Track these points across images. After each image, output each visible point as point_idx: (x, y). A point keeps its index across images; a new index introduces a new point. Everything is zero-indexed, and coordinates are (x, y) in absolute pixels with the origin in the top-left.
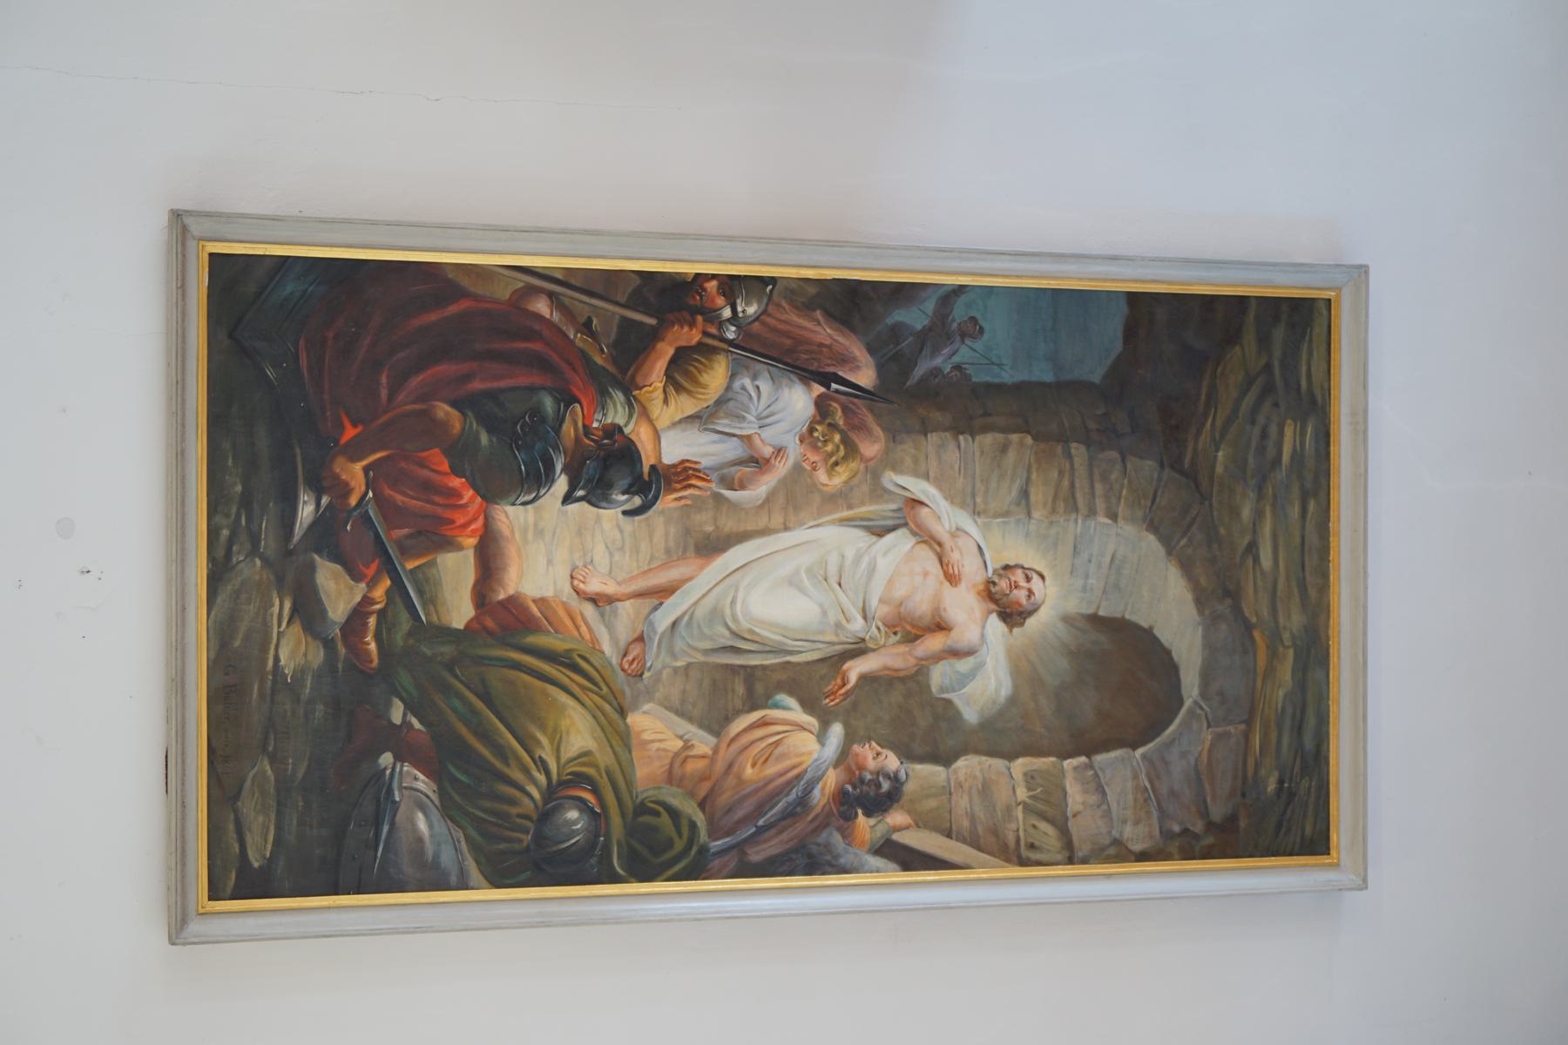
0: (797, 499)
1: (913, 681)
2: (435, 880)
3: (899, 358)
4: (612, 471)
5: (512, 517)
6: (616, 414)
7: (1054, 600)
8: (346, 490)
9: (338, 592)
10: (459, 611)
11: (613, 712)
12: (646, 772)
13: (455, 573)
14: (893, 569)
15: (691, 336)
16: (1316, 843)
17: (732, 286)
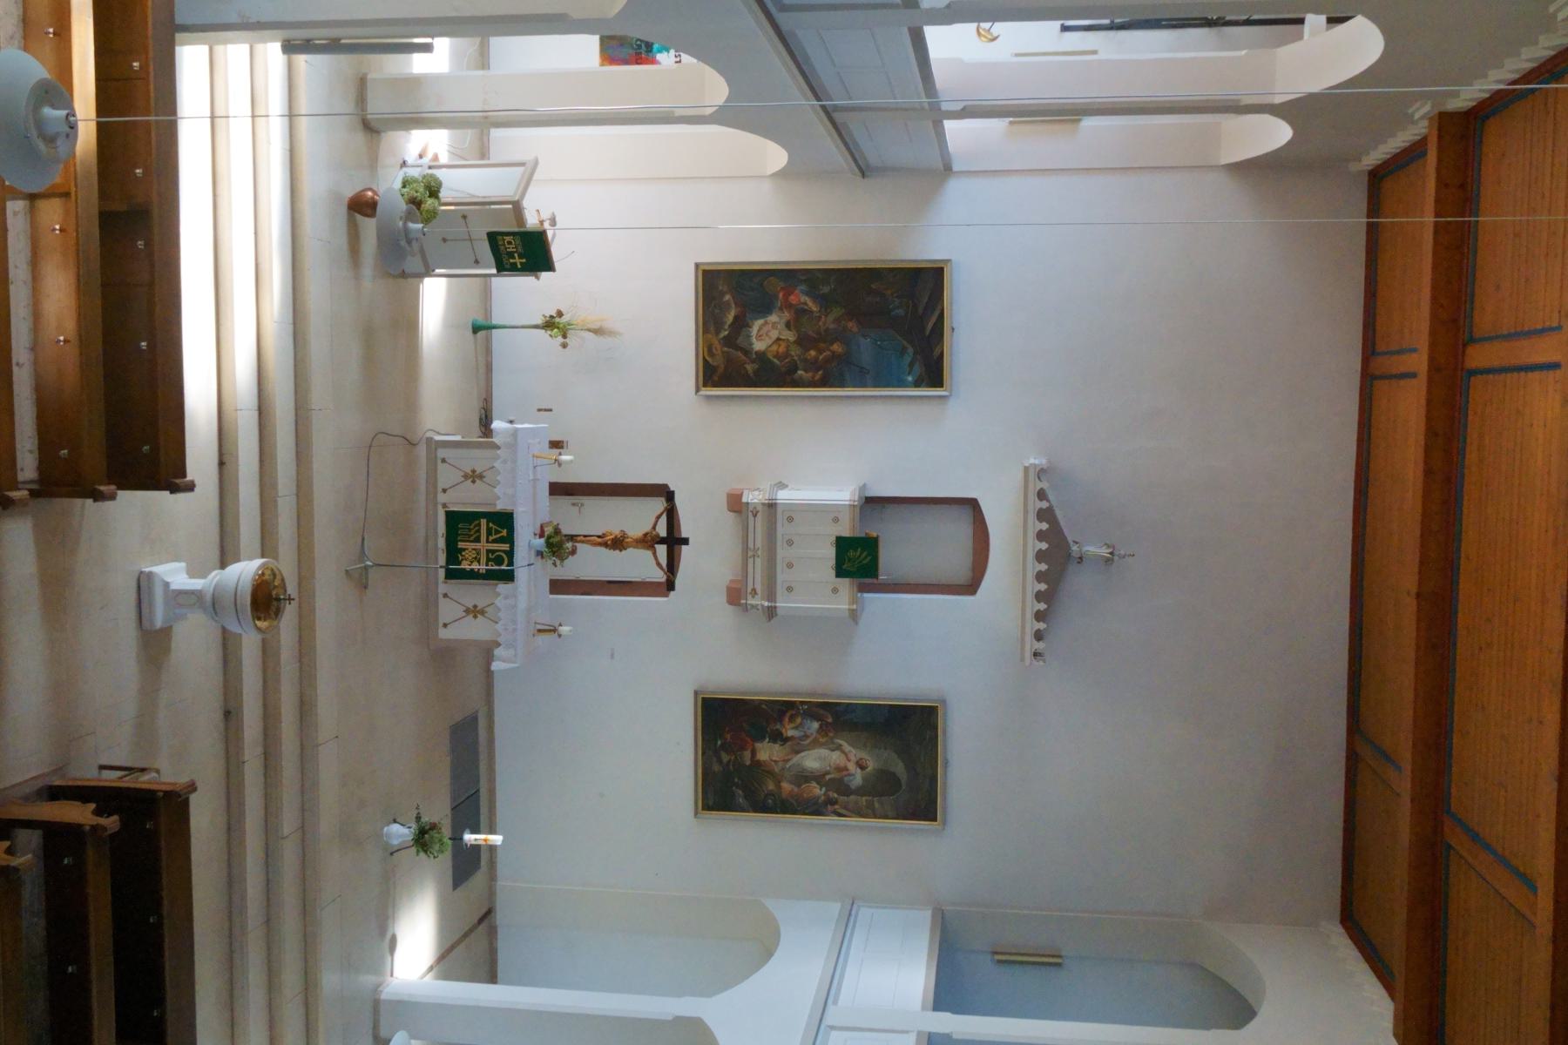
0: (815, 744)
1: (841, 780)
2: (743, 810)
3: (839, 718)
4: (778, 737)
5: (758, 745)
7: (871, 765)
12: (784, 795)
14: (836, 758)
16: (932, 817)
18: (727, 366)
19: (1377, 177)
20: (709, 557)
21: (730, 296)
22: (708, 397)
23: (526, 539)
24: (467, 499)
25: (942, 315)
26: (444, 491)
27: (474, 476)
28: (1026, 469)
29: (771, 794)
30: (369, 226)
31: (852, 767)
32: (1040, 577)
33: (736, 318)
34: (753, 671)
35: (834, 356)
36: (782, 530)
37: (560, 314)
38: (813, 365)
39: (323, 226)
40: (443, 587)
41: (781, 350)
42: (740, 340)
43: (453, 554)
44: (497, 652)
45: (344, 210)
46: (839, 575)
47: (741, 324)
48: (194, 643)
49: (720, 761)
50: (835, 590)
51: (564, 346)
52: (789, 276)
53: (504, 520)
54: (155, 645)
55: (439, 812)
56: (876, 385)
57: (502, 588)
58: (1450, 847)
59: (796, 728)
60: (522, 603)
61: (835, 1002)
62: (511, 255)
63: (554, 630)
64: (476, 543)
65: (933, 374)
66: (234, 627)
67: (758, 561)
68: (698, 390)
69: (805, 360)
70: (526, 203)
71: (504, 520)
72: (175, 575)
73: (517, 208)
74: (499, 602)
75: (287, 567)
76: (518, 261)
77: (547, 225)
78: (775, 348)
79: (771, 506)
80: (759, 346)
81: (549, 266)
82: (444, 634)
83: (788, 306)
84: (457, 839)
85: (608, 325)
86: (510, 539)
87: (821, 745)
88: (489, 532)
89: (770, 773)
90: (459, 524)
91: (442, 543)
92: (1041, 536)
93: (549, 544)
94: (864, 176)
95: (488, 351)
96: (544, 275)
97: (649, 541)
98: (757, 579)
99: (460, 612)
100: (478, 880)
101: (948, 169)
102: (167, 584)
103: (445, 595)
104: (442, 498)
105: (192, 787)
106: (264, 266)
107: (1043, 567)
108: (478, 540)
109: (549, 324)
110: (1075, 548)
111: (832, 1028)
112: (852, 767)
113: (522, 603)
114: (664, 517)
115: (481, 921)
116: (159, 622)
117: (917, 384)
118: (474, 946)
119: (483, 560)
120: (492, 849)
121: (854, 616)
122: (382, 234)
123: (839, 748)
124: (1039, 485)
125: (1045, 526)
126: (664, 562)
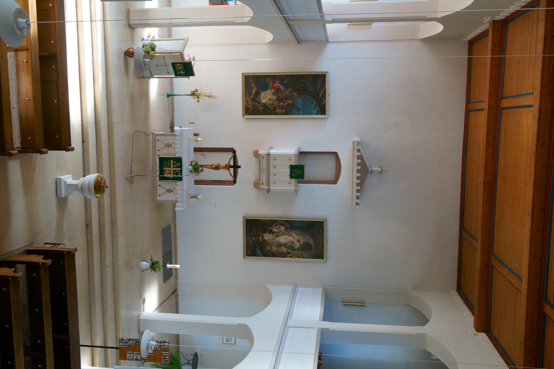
0: (283, 234)
2: (260, 256)
3: (291, 225)
4: (271, 232)
5: (264, 235)
9: (253, 239)
10: (261, 240)
11: (271, 246)
12: (273, 251)
13: (261, 238)
14: (290, 238)
18: (253, 108)
19: (471, 43)
20: (248, 172)
21: (254, 84)
22: (247, 118)
23: (186, 166)
24: (166, 153)
26: (159, 150)
27: (168, 146)
28: (354, 142)
29: (268, 251)
30: (131, 61)
31: (296, 241)
32: (358, 178)
33: (256, 92)
34: (262, 210)
35: (289, 104)
36: (272, 163)
37: (197, 91)
38: (282, 107)
39: (116, 60)
40: (158, 183)
41: (271, 102)
42: (258, 99)
43: (162, 172)
44: (177, 204)
45: (123, 55)
46: (291, 177)
47: (257, 94)
48: (75, 202)
49: (252, 240)
50: (290, 183)
51: (198, 101)
52: (273, 78)
53: (179, 160)
54: (62, 202)
55: (158, 257)
56: (303, 114)
57: (178, 183)
58: (493, 266)
60: (185, 188)
61: (291, 319)
62: (180, 71)
63: (196, 197)
64: (170, 168)
65: (322, 110)
66: (88, 196)
67: (264, 173)
68: (243, 116)
69: (279, 106)
70: (184, 53)
71: (179, 160)
72: (68, 179)
73: (182, 54)
74: (177, 188)
75: (106, 176)
76: (182, 72)
77: (192, 60)
78: (269, 102)
79: (268, 155)
80: (264, 101)
81: (193, 74)
82: (159, 198)
83: (273, 87)
84: (165, 266)
85: (213, 94)
86: (181, 167)
87: (286, 234)
88: (174, 164)
89: (269, 244)
90: (164, 161)
91: (158, 168)
92: (358, 164)
93: (194, 168)
94: (299, 43)
95: (172, 103)
96: (191, 77)
97: (227, 167)
98: (264, 180)
99: (164, 191)
100: (172, 279)
101: (327, 41)
102: (66, 182)
103: (159, 186)
104: (158, 153)
105: (76, 250)
106: (96, 74)
107: (359, 175)
108: (170, 167)
109: (193, 94)
110: (370, 168)
111: (290, 327)
112: (296, 241)
113: (185, 188)
114: (232, 160)
115: (173, 293)
116: (63, 195)
117: (317, 114)
118: (171, 301)
119: (172, 174)
120: (176, 269)
121: (296, 191)
122: (137, 63)
123: (291, 235)
124: (358, 147)
125: (360, 161)
126: (232, 174)
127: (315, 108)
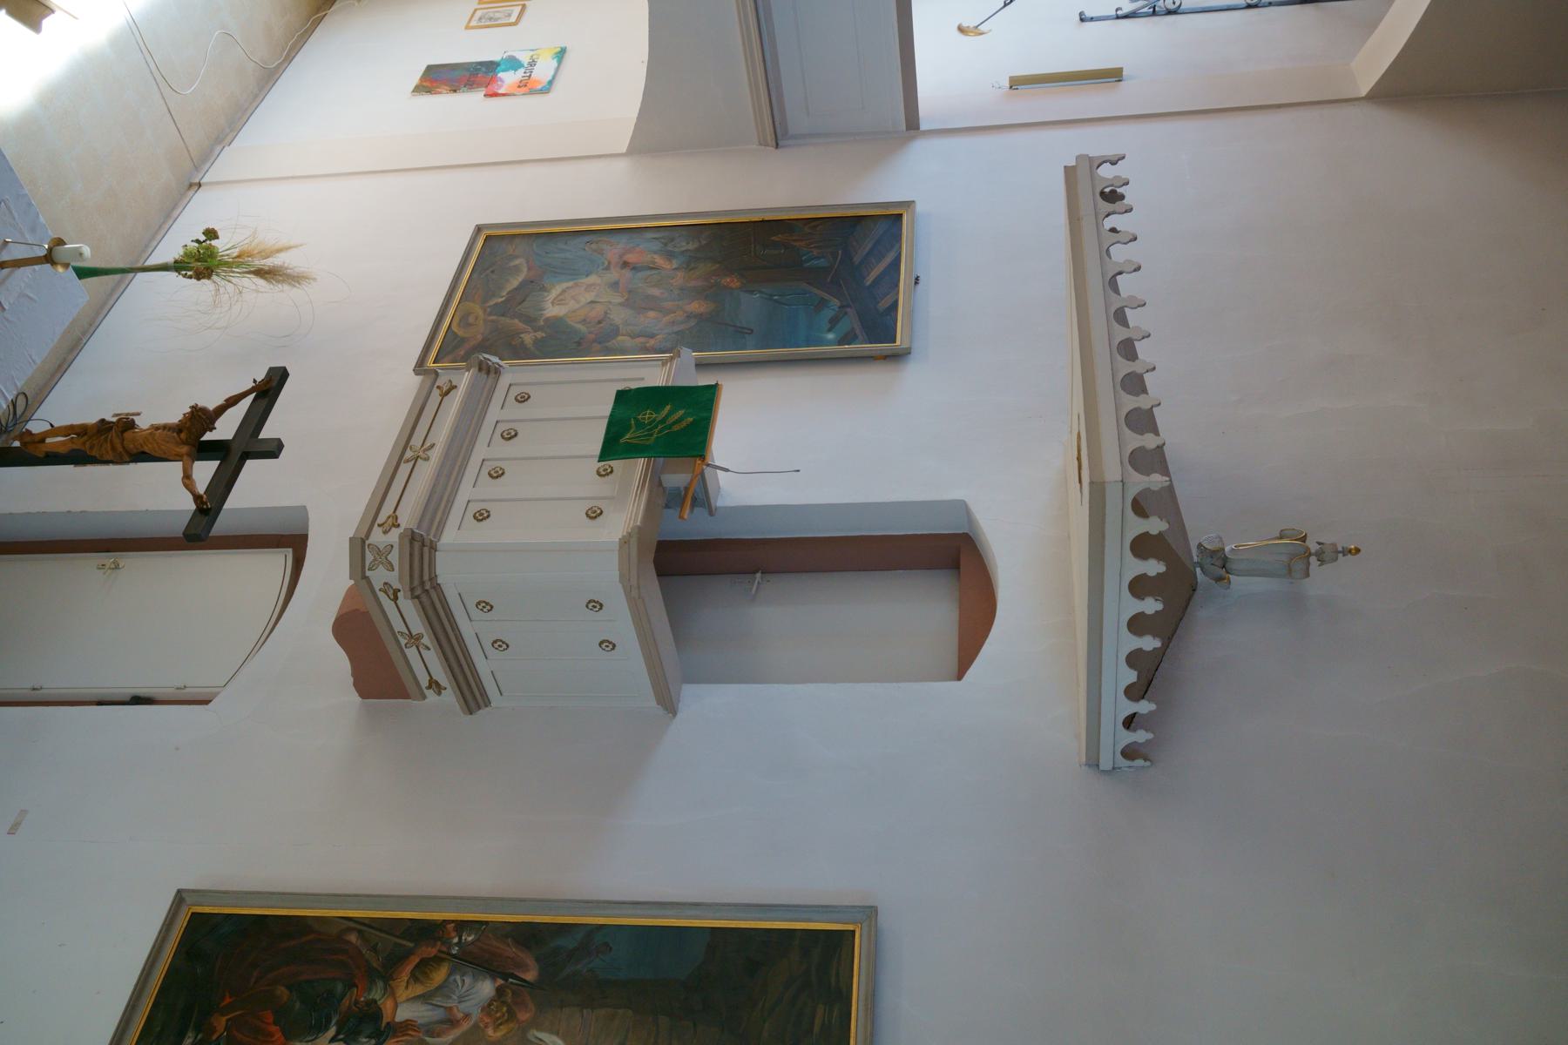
6: (376, 994)
8: (214, 1030)
15: (430, 951)
17: (462, 926)
25: (896, 264)
59: (425, 998)
80: (552, 311)
94: (777, 146)
127: (833, 322)
